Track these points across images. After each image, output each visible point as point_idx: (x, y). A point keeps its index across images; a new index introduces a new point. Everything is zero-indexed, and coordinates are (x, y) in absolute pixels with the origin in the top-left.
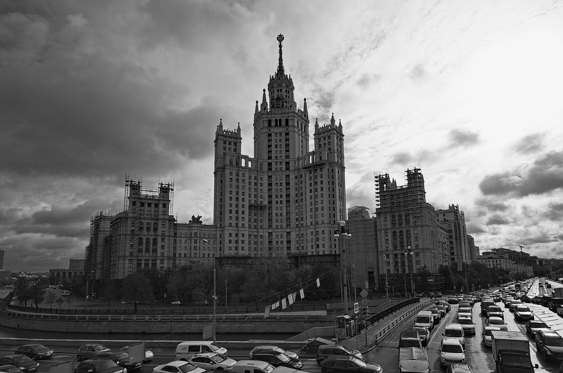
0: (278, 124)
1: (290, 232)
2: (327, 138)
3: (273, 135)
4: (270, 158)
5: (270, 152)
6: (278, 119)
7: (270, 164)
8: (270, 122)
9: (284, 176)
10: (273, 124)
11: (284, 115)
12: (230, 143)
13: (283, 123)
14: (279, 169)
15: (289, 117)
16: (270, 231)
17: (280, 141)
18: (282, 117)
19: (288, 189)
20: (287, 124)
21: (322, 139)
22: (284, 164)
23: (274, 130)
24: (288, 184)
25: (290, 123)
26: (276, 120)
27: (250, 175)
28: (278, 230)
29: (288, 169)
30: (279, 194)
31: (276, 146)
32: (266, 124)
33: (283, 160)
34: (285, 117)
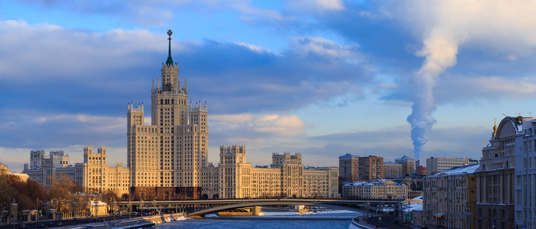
0: (167, 103)
1: (173, 172)
2: (196, 116)
3: (164, 110)
4: (162, 124)
6: (167, 100)
7: (162, 129)
8: (162, 100)
9: (170, 137)
10: (164, 102)
12: (137, 117)
13: (170, 102)
16: (162, 170)
17: (168, 114)
19: (173, 145)
20: (173, 103)
21: (193, 116)
22: (170, 129)
24: (173, 142)
25: (175, 102)
28: (166, 170)
29: (173, 132)
30: (167, 148)
31: (166, 117)
32: (159, 102)
34: (171, 98)
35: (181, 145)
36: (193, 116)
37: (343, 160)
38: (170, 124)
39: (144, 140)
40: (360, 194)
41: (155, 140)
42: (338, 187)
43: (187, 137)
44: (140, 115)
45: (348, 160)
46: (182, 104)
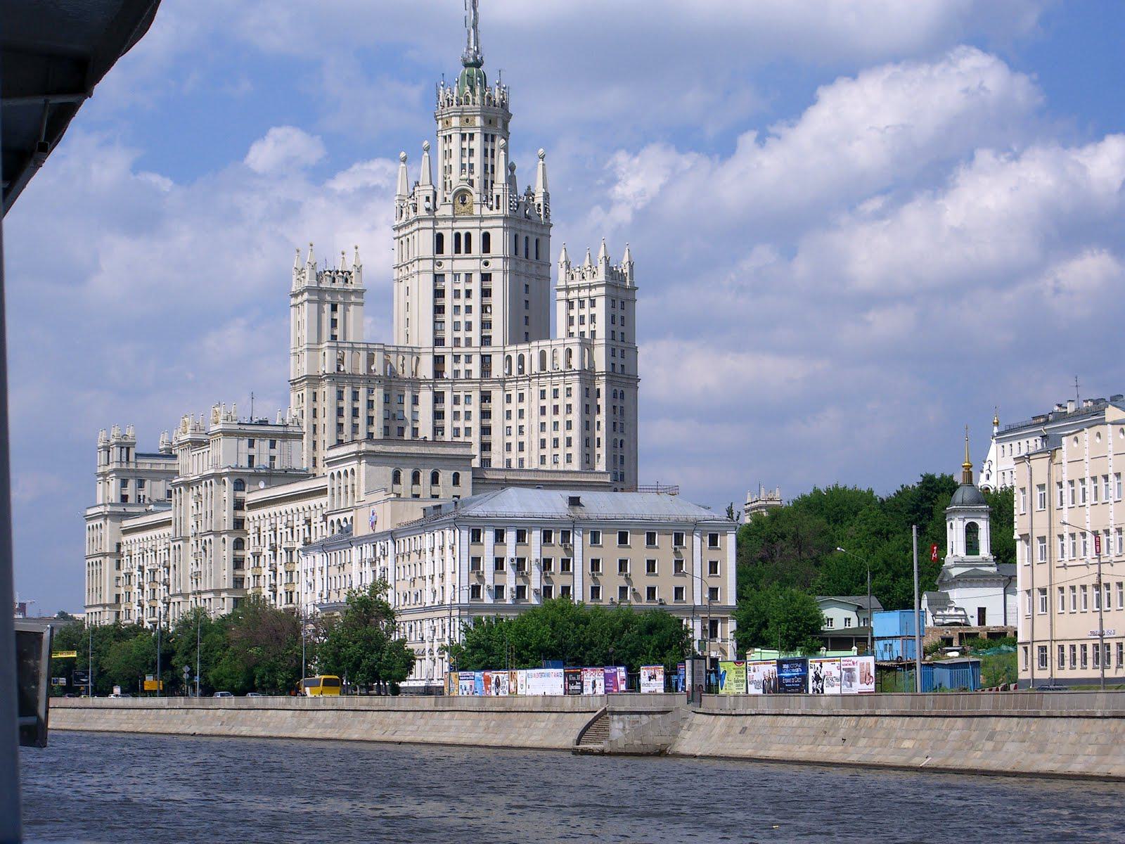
3: (448, 277)
5: (437, 324)
6: (463, 233)
8: (439, 239)
9: (476, 396)
11: (476, 224)
14: (462, 376)
20: (486, 247)
21: (576, 303)
22: (476, 360)
23: (454, 264)
24: (486, 414)
26: (458, 236)
27: (388, 392)
33: (473, 350)
34: (481, 228)
35: (521, 427)
36: (576, 303)
38: (476, 341)
43: (549, 394)
46: (527, 257)
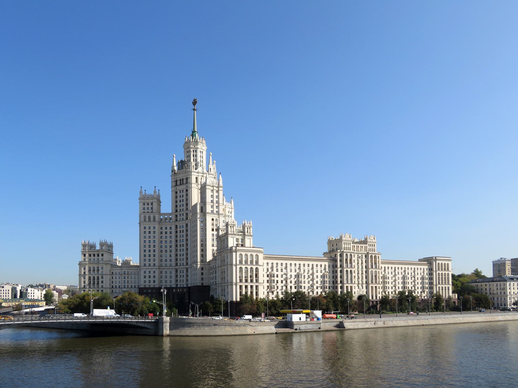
3: (178, 192)
4: (176, 211)
6: (181, 179)
7: (176, 216)
9: (185, 225)
14: (182, 219)
15: (187, 176)
18: (183, 176)
20: (187, 183)
22: (185, 215)
32: (174, 184)
34: (185, 176)
37: (497, 264)
39: (152, 230)
40: (490, 293)
41: (168, 231)
42: (451, 283)
44: (151, 201)
45: (501, 264)
